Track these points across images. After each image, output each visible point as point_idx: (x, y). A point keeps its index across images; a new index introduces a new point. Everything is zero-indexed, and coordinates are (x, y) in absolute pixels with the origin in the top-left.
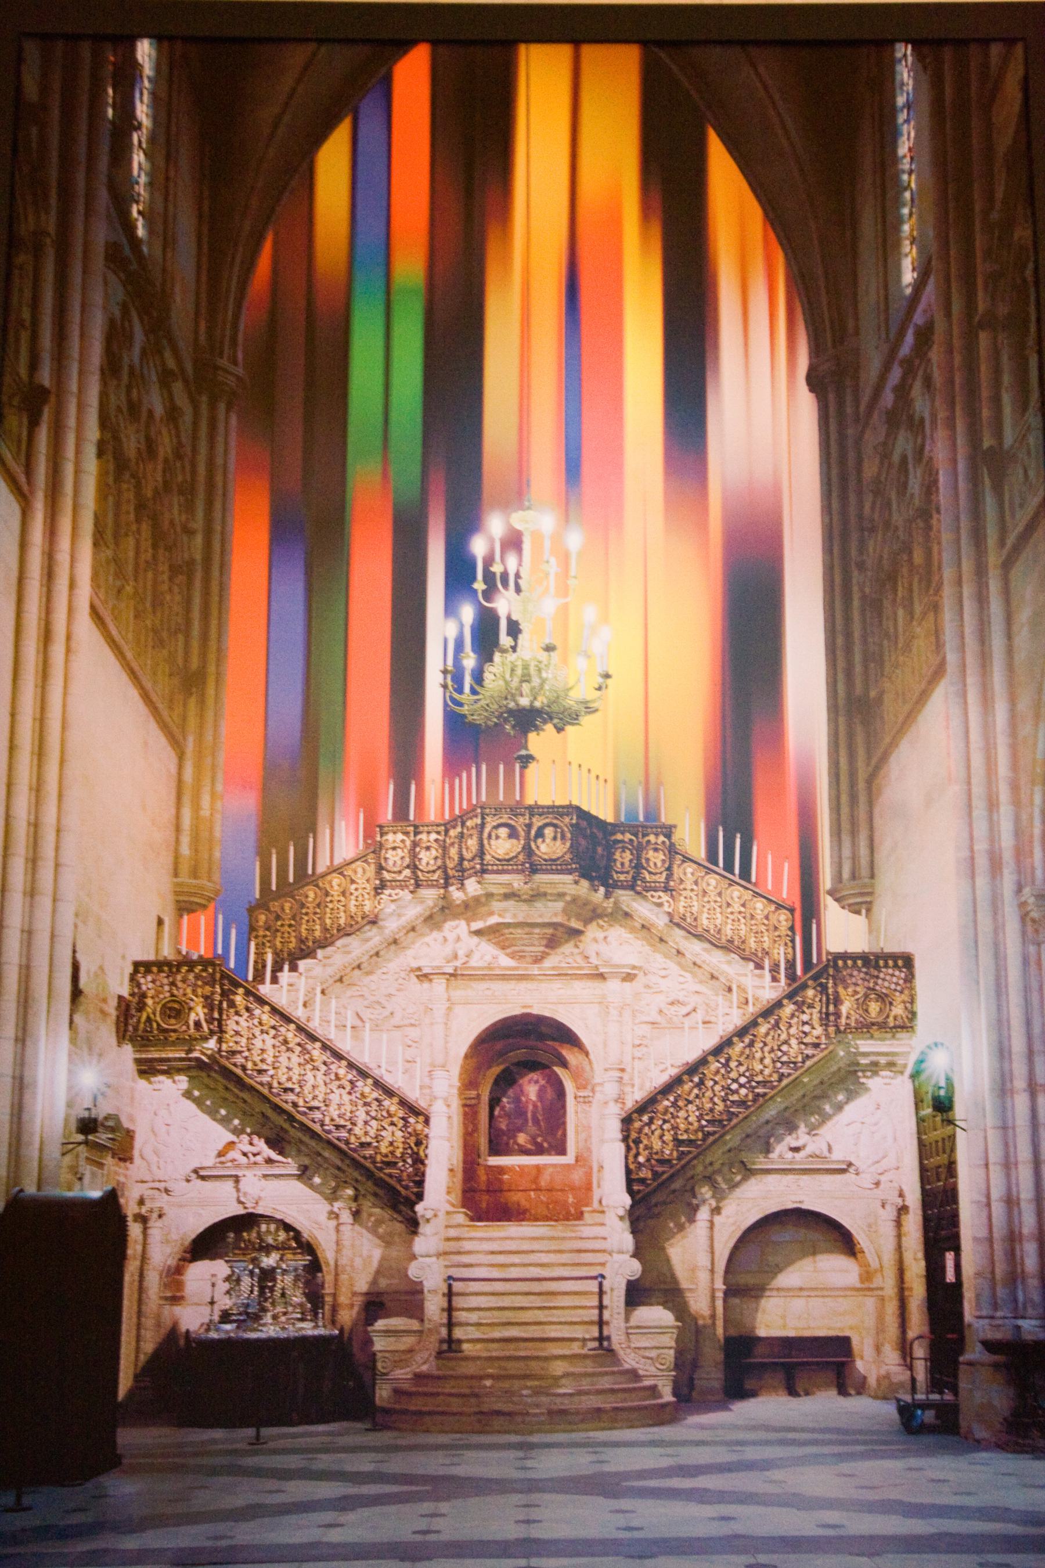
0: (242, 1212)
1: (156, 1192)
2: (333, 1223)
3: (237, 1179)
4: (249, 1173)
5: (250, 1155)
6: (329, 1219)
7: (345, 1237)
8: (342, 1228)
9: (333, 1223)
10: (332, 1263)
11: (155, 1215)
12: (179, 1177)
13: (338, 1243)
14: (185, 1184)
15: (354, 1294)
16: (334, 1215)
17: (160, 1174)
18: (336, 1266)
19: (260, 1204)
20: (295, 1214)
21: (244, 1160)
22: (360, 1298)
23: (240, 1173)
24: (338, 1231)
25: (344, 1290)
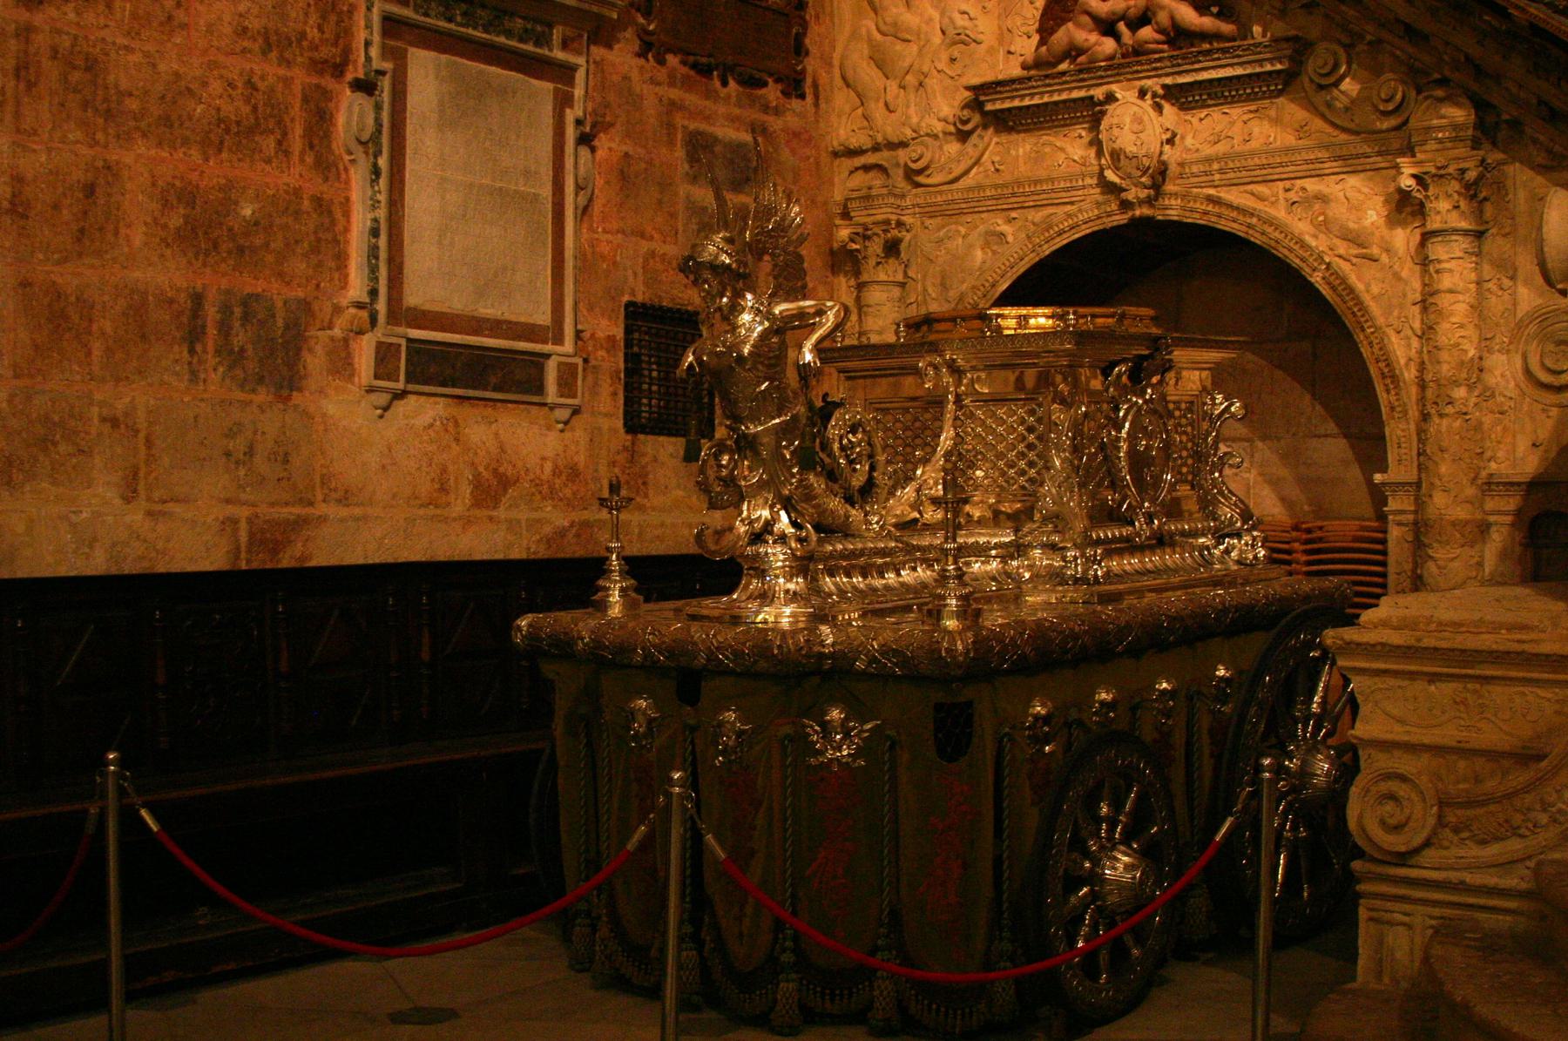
0: (1121, 219)
1: (876, 180)
2: (1403, 239)
3: (1092, 113)
4: (1125, 93)
5: (1122, 26)
6: (1393, 221)
7: (1446, 282)
8: (1437, 250)
9: (1403, 239)
10: (1410, 375)
11: (876, 247)
12: (938, 127)
13: (1426, 303)
14: (953, 147)
15: (1490, 486)
16: (1405, 207)
17: (889, 128)
18: (1422, 385)
19: (1169, 187)
20: (1280, 213)
21: (1109, 45)
22: (1512, 503)
23: (1099, 93)
24: (1424, 262)
25: (1443, 469)
